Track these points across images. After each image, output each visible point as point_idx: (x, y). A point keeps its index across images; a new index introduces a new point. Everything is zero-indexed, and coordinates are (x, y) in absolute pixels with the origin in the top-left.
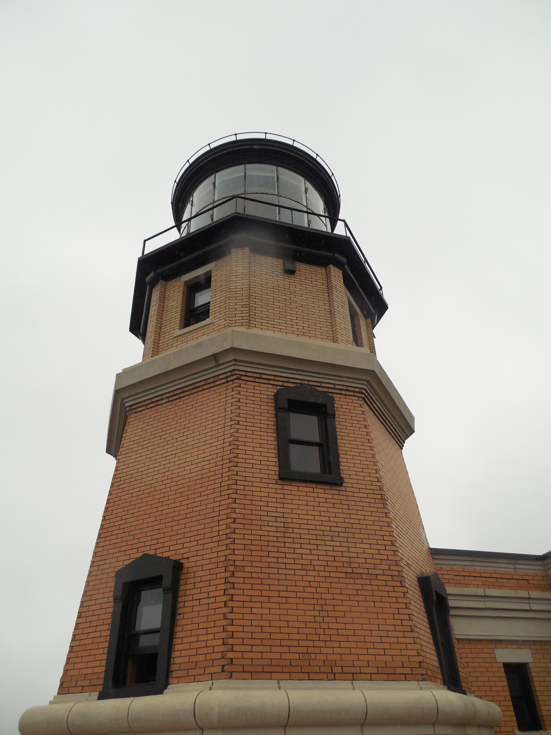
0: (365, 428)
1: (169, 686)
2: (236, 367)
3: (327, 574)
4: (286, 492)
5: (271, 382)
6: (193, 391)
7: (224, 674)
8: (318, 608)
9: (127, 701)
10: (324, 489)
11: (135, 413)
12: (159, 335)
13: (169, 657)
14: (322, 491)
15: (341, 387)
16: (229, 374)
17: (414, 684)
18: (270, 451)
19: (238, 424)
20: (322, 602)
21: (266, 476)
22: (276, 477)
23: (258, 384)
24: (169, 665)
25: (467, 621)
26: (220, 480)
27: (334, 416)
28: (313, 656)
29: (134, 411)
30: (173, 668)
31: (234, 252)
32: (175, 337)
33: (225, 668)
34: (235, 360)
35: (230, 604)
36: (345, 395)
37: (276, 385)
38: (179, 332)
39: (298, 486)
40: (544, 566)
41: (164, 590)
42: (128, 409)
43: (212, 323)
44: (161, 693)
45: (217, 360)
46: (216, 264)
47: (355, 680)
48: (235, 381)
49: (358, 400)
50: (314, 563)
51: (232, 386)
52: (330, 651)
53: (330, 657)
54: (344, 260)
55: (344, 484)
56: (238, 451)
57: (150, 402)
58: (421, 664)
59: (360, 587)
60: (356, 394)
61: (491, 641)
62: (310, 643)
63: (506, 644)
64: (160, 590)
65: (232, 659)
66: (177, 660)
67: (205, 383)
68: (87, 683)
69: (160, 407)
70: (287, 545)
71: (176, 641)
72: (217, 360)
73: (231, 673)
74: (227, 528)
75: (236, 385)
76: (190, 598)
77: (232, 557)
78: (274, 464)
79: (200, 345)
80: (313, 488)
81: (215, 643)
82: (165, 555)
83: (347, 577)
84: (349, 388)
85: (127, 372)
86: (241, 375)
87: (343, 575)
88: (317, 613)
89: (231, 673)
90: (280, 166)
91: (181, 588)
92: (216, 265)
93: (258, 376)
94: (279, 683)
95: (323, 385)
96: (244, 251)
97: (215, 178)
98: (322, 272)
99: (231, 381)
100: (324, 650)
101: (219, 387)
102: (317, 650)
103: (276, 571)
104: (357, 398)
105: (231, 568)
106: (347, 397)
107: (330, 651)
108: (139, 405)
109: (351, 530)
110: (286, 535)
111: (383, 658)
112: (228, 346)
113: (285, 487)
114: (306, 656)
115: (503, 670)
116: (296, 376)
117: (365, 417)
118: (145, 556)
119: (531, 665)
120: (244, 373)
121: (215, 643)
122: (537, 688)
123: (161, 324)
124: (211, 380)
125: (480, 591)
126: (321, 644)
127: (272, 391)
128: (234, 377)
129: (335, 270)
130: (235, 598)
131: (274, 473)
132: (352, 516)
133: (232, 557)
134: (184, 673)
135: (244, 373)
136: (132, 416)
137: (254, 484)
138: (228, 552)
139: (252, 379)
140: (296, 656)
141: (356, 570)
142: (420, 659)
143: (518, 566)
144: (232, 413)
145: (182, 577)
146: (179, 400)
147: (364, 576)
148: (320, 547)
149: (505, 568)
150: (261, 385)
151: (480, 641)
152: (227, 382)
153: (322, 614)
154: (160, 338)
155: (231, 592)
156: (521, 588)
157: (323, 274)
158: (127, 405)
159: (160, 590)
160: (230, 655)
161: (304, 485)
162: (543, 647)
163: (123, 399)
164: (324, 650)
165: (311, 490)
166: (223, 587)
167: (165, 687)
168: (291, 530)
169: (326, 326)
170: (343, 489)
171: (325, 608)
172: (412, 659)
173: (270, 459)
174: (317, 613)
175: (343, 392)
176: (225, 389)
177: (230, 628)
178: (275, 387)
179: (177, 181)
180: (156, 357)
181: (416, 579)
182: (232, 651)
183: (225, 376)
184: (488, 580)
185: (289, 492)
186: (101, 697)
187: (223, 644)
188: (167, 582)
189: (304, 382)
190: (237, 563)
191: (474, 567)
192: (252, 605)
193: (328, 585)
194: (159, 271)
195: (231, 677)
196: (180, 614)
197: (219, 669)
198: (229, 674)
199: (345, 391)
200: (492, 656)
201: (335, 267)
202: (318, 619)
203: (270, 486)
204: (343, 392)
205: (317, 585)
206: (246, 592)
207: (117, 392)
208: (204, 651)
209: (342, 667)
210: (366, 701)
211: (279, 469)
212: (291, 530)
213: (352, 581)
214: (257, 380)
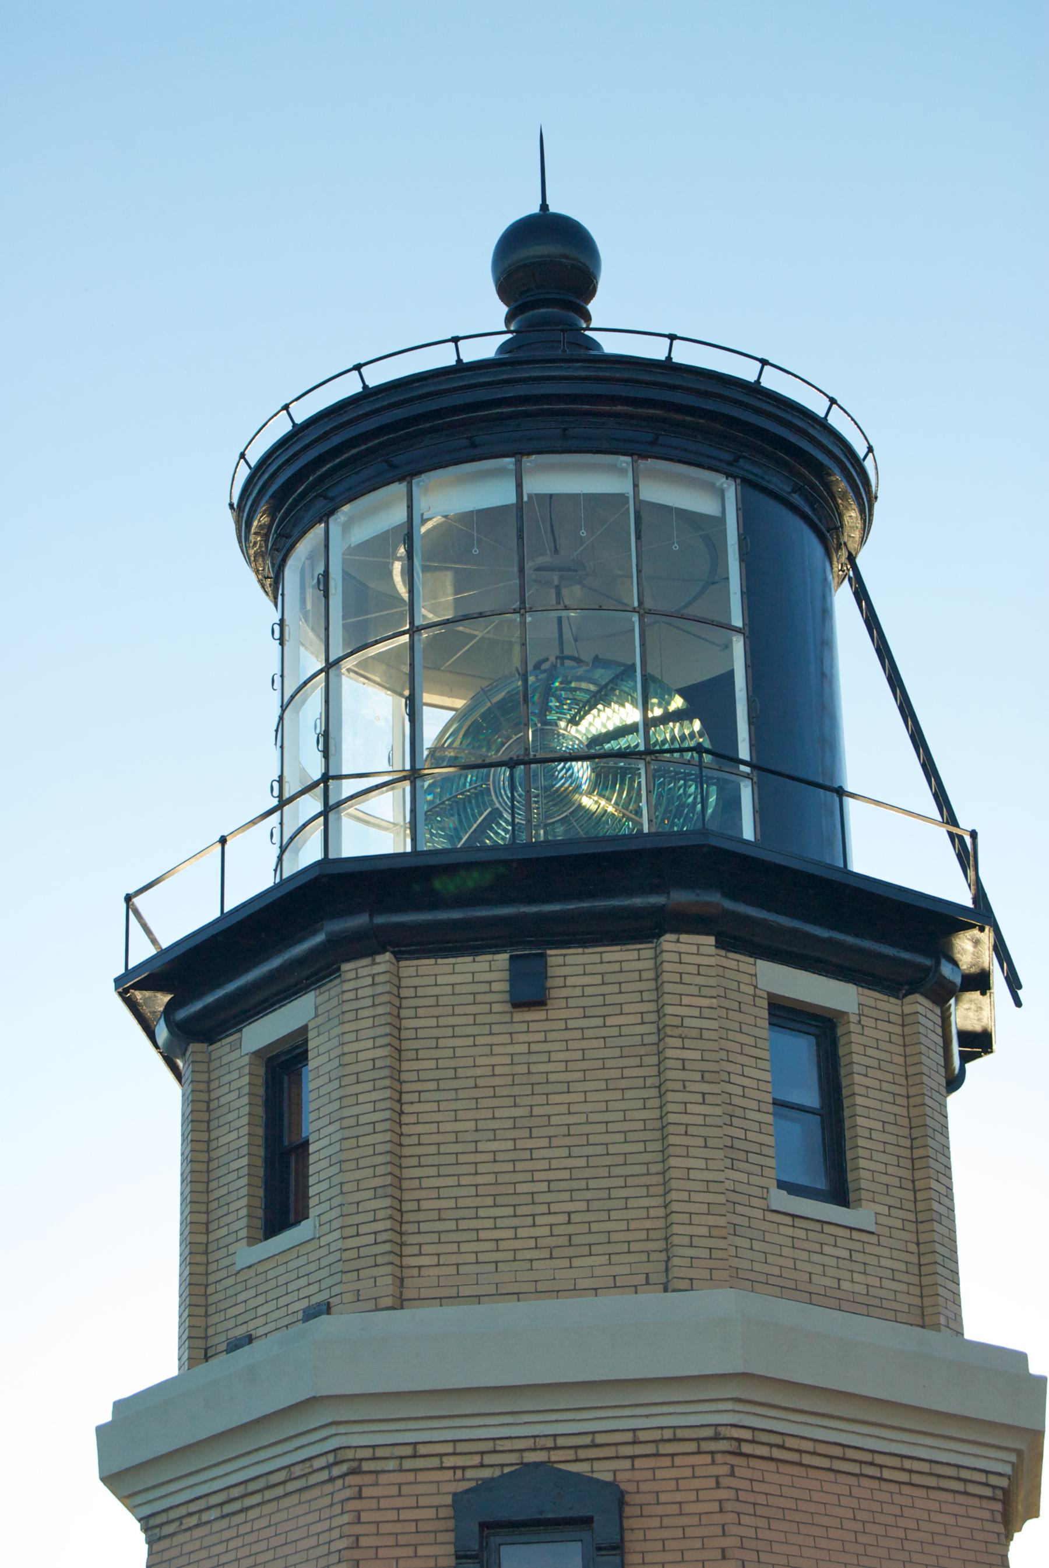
5: (449, 1462)
12: (206, 1253)
15: (657, 1435)
16: (331, 1458)
23: (410, 1477)
38: (246, 1255)
46: (319, 1000)
49: (713, 1463)
75: (348, 1493)
92: (316, 1008)
96: (376, 969)
98: (640, 965)
104: (708, 1459)
106: (678, 1461)
123: (207, 1213)
124: (297, 1471)
128: (344, 1468)
135: (368, 1453)
146: (241, 1517)
150: (422, 1476)
152: (332, 1480)
169: (643, 1191)
176: (327, 1501)
201: (684, 937)
214: (407, 1464)
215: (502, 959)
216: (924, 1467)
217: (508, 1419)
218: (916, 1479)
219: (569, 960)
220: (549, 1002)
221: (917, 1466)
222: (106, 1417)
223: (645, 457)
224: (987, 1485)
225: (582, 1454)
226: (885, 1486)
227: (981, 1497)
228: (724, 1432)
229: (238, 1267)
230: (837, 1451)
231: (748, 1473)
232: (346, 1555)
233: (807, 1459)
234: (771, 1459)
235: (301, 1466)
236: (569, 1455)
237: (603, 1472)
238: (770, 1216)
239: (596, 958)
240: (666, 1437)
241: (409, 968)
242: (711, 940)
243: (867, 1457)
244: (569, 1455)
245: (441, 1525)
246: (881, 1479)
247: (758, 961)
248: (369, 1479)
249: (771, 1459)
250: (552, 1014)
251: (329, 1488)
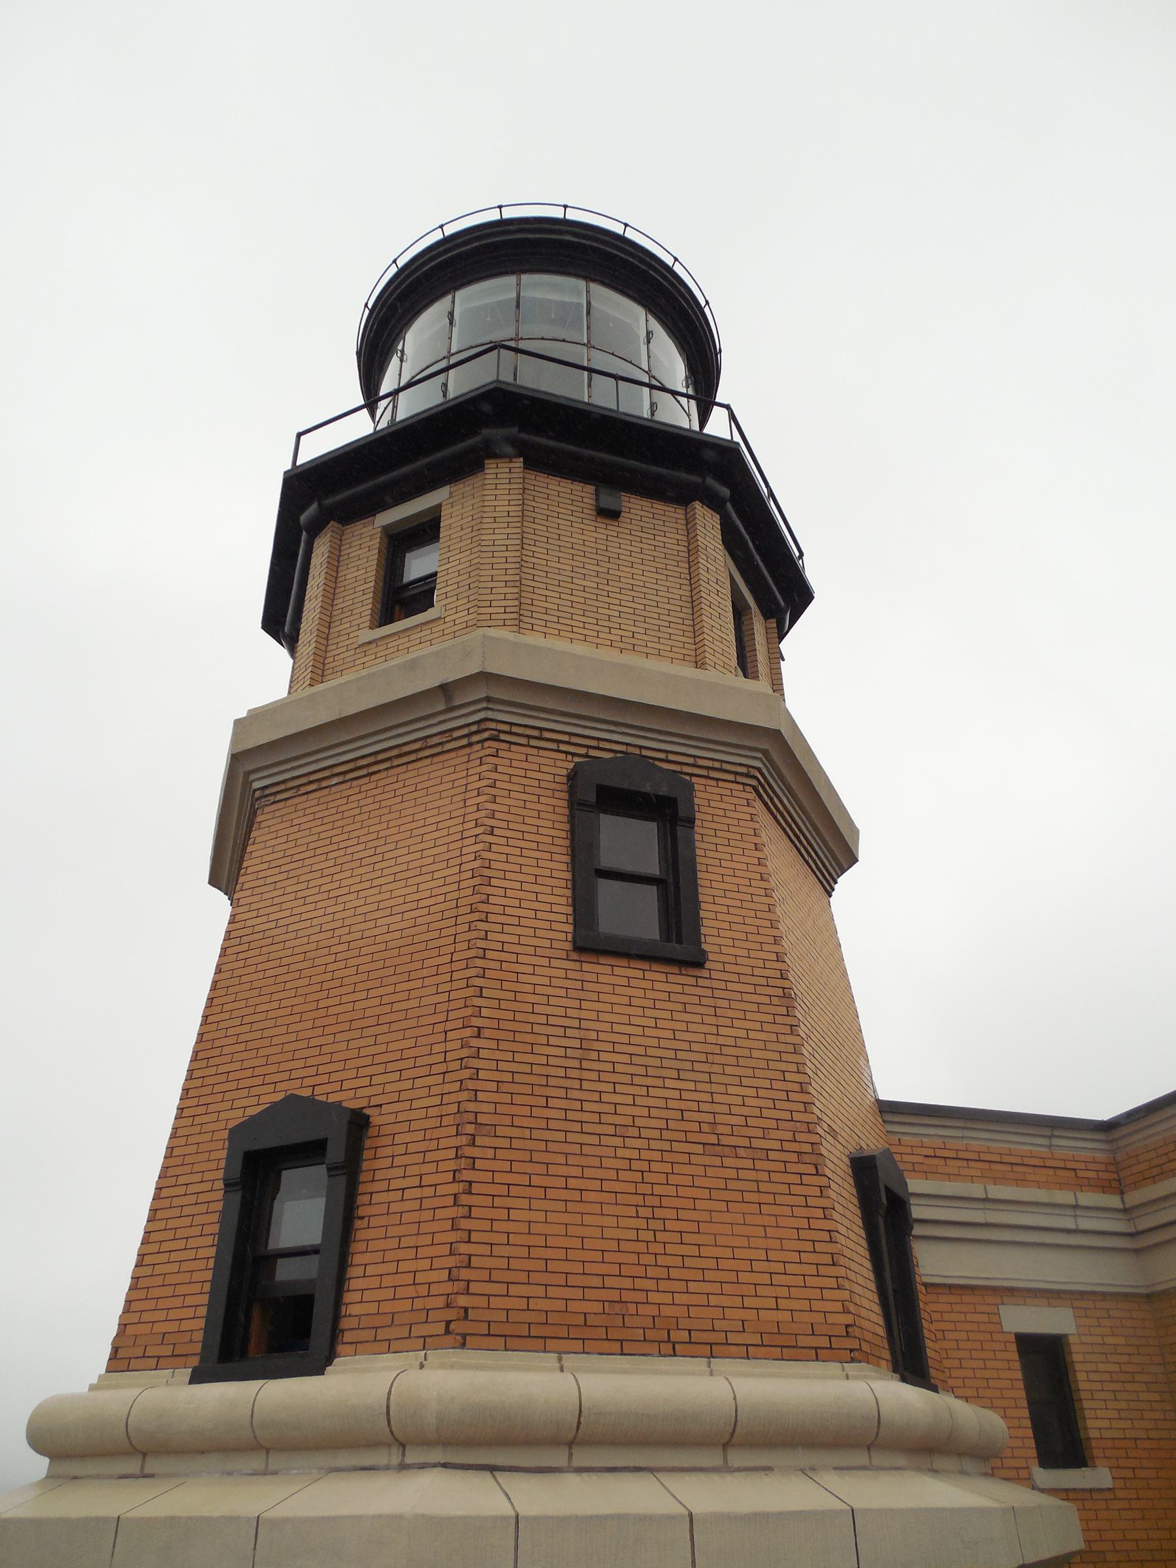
0: (756, 849)
1: (336, 1360)
2: (490, 714)
3: (666, 1146)
4: (587, 977)
5: (563, 747)
6: (396, 762)
7: (449, 1339)
8: (644, 1212)
9: (252, 1386)
10: (667, 973)
11: (274, 803)
12: (327, 639)
13: (338, 1303)
14: (662, 977)
16: (474, 728)
17: (834, 1368)
18: (556, 891)
19: (492, 834)
20: (655, 1201)
21: (547, 943)
22: (569, 946)
23: (535, 751)
24: (336, 1317)
25: (945, 1249)
26: (451, 949)
27: (690, 822)
28: (632, 1309)
29: (272, 799)
30: (344, 1324)
31: (490, 466)
32: (360, 646)
33: (452, 1326)
34: (488, 699)
35: (465, 1199)
36: (717, 780)
37: (573, 754)
39: (612, 966)
40: (1109, 1142)
41: (329, 1169)
42: (258, 794)
43: (439, 618)
44: (320, 1372)
45: (448, 698)
46: (452, 490)
47: (714, 1357)
48: (486, 744)
49: (744, 791)
50: (638, 1122)
51: (481, 754)
52: (667, 1298)
53: (667, 1311)
54: (725, 492)
55: (708, 965)
56: (489, 890)
57: (304, 780)
58: (850, 1330)
59: (732, 1173)
60: (740, 779)
61: (994, 1290)
62: (628, 1283)
64: (322, 1169)
65: (466, 1309)
66: (354, 1310)
67: (423, 746)
68: (167, 1351)
69: (327, 791)
70: (585, 1085)
71: (353, 1272)
72: (448, 698)
73: (464, 1336)
74: (462, 1047)
75: (488, 752)
76: (383, 1186)
77: (472, 1107)
78: (563, 918)
79: (413, 665)
80: (644, 970)
81: (433, 1276)
82: (332, 1099)
83: (707, 1153)
84: (725, 766)
85: (257, 717)
86: (500, 731)
87: (699, 1149)
88: (642, 1224)
89: (464, 1336)
90: (594, 281)
91: (365, 1165)
92: (451, 493)
93: (536, 733)
94: (560, 1359)
95: (671, 757)
96: (512, 465)
97: (453, 302)
99: (478, 742)
100: (653, 1297)
101: (453, 755)
102: (641, 1297)
103: (560, 1136)
104: (741, 787)
105: (470, 1129)
106: (721, 784)
107: (667, 1298)
108: (282, 787)
109: (717, 1059)
110: (585, 1065)
112: (473, 669)
113: (586, 967)
114: (617, 1308)
115: (1014, 1347)
116: (615, 737)
117: (757, 826)
118: (292, 1100)
119: (1071, 1340)
120: (506, 728)
121: (433, 1276)
122: (1082, 1386)
123: (331, 617)
124: (436, 740)
125: (976, 1190)
126: (649, 1284)
127: (564, 766)
128: (486, 735)
129: (705, 513)
130: (476, 1188)
131: (562, 936)
132: (722, 1031)
133: (472, 1107)
134: (368, 1335)
135: (506, 728)
136: (267, 810)
137: (521, 959)
138: (464, 1096)
139: (523, 741)
140: (597, 1307)
141: (725, 1140)
142: (849, 1319)
143: (1056, 1142)
144: (478, 810)
145: (368, 1143)
146: (366, 780)
147: (742, 1152)
148: (652, 1091)
149: (1032, 1145)
150: (542, 753)
151: (972, 1289)
152: (470, 745)
153: (654, 1224)
154: (328, 645)
155: (467, 1175)
156: (1062, 1186)
157: (683, 587)
158: (256, 785)
159: (322, 1169)
160: (463, 1301)
161: (624, 963)
162: (1099, 1305)
163: (248, 774)
164: (653, 1297)
165: (640, 974)
166: (452, 1165)
167: (329, 1361)
168: (594, 1055)
170: (705, 973)
171: (659, 1213)
172: (831, 1318)
173: (555, 908)
174: (642, 1224)
175: (713, 774)
177: (464, 1248)
178: (570, 757)
179: (370, 306)
180: (320, 687)
181: (847, 1161)
182: (467, 1292)
183: (465, 731)
184: (994, 1166)
185: (593, 977)
186: (197, 1377)
187: (450, 1279)
188: (336, 1152)
189: (631, 750)
190: (481, 1119)
191: (965, 1141)
192: (509, 1202)
193: (667, 1168)
194: (330, 501)
195: (463, 1345)
196: (362, 1218)
197: (440, 1328)
198: (459, 1338)
199: (715, 772)
200: (994, 1319)
202: (644, 1235)
203: (554, 963)
204: (713, 774)
205: (644, 1166)
206: (499, 1178)
207: (236, 759)
208: (411, 1291)
209: (690, 1331)
210: (735, 1398)
211: (575, 930)
212: (594, 1055)
213: (717, 1161)
214: (533, 742)
215: (590, 489)
217: (612, 728)
220: (621, 519)
222: (243, 714)
229: (360, 643)
232: (487, 790)
235: (439, 737)
239: (650, 505)
240: (715, 766)
241: (531, 475)
245: (558, 787)
248: (506, 746)
251: (467, 751)
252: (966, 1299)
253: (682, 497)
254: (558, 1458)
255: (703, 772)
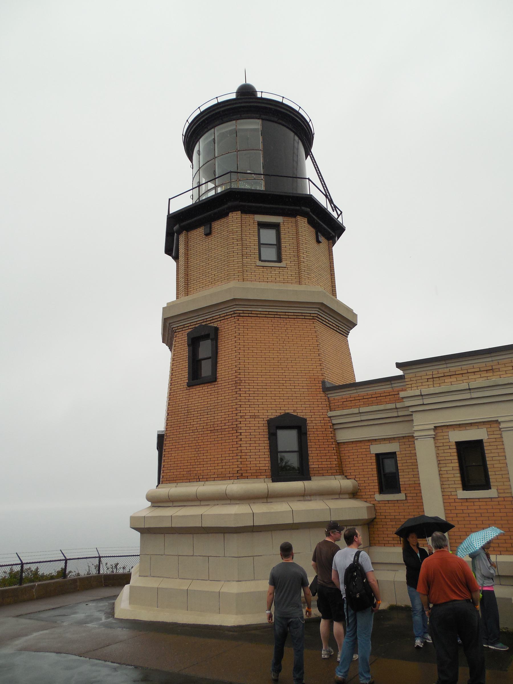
15: (223, 315)
22: (186, 386)
55: (218, 380)
61: (369, 441)
63: (389, 441)
95: (214, 318)
102: (194, 469)
111: (221, 470)
113: (190, 390)
115: (374, 458)
119: (397, 453)
125: (356, 410)
139: (181, 330)
151: (361, 441)
165: (201, 388)
170: (217, 383)
172: (234, 469)
181: (267, 422)
199: (224, 318)
201: (233, 213)
216: (292, 314)
217: (198, 317)
218: (290, 317)
219: (216, 223)
221: (289, 314)
223: (238, 120)
224: (310, 316)
225: (212, 321)
226: (281, 319)
227: (310, 319)
228: (235, 312)
230: (267, 313)
231: (243, 320)
233: (258, 315)
234: (249, 316)
236: (209, 322)
237: (215, 325)
238: (256, 267)
241: (189, 233)
242: (240, 212)
243: (276, 313)
244: (209, 322)
246: (280, 318)
247: (255, 215)
249: (249, 316)
250: (212, 235)
252: (358, 445)
253: (224, 214)
254: (171, 504)
255: (223, 318)
